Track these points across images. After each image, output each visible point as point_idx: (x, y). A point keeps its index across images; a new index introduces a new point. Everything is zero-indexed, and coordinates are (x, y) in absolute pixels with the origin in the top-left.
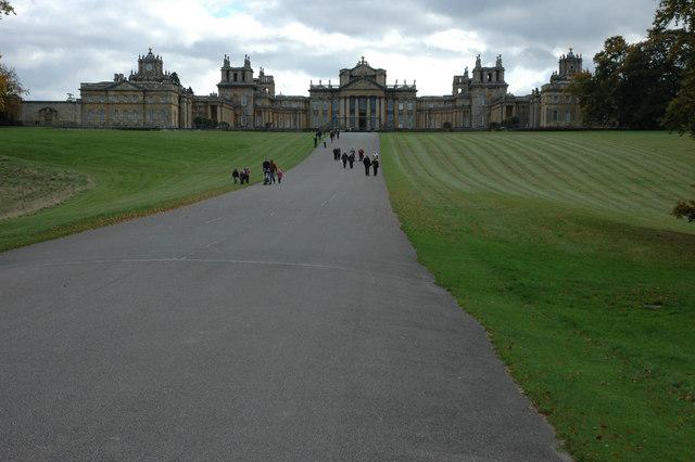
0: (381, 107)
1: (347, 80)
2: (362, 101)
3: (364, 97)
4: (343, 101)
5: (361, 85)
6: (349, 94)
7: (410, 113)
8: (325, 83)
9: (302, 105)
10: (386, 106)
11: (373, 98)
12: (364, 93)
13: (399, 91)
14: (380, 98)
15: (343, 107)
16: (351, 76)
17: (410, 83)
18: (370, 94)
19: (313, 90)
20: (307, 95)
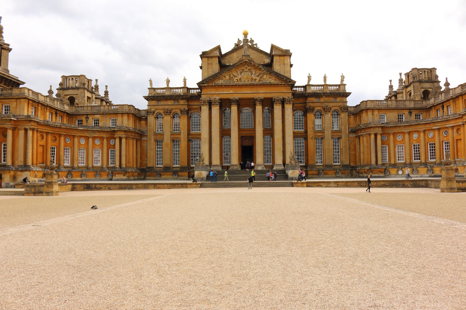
0: (286, 120)
1: (216, 68)
2: (247, 110)
3: (251, 103)
4: (205, 109)
5: (244, 76)
6: (216, 94)
7: (337, 136)
8: (177, 83)
9: (127, 123)
10: (295, 124)
11: (269, 103)
12: (247, 93)
13: (316, 95)
14: (283, 102)
15: (207, 121)
16: (223, 67)
17: (334, 80)
18: (262, 93)
19: (154, 97)
20: (143, 105)
